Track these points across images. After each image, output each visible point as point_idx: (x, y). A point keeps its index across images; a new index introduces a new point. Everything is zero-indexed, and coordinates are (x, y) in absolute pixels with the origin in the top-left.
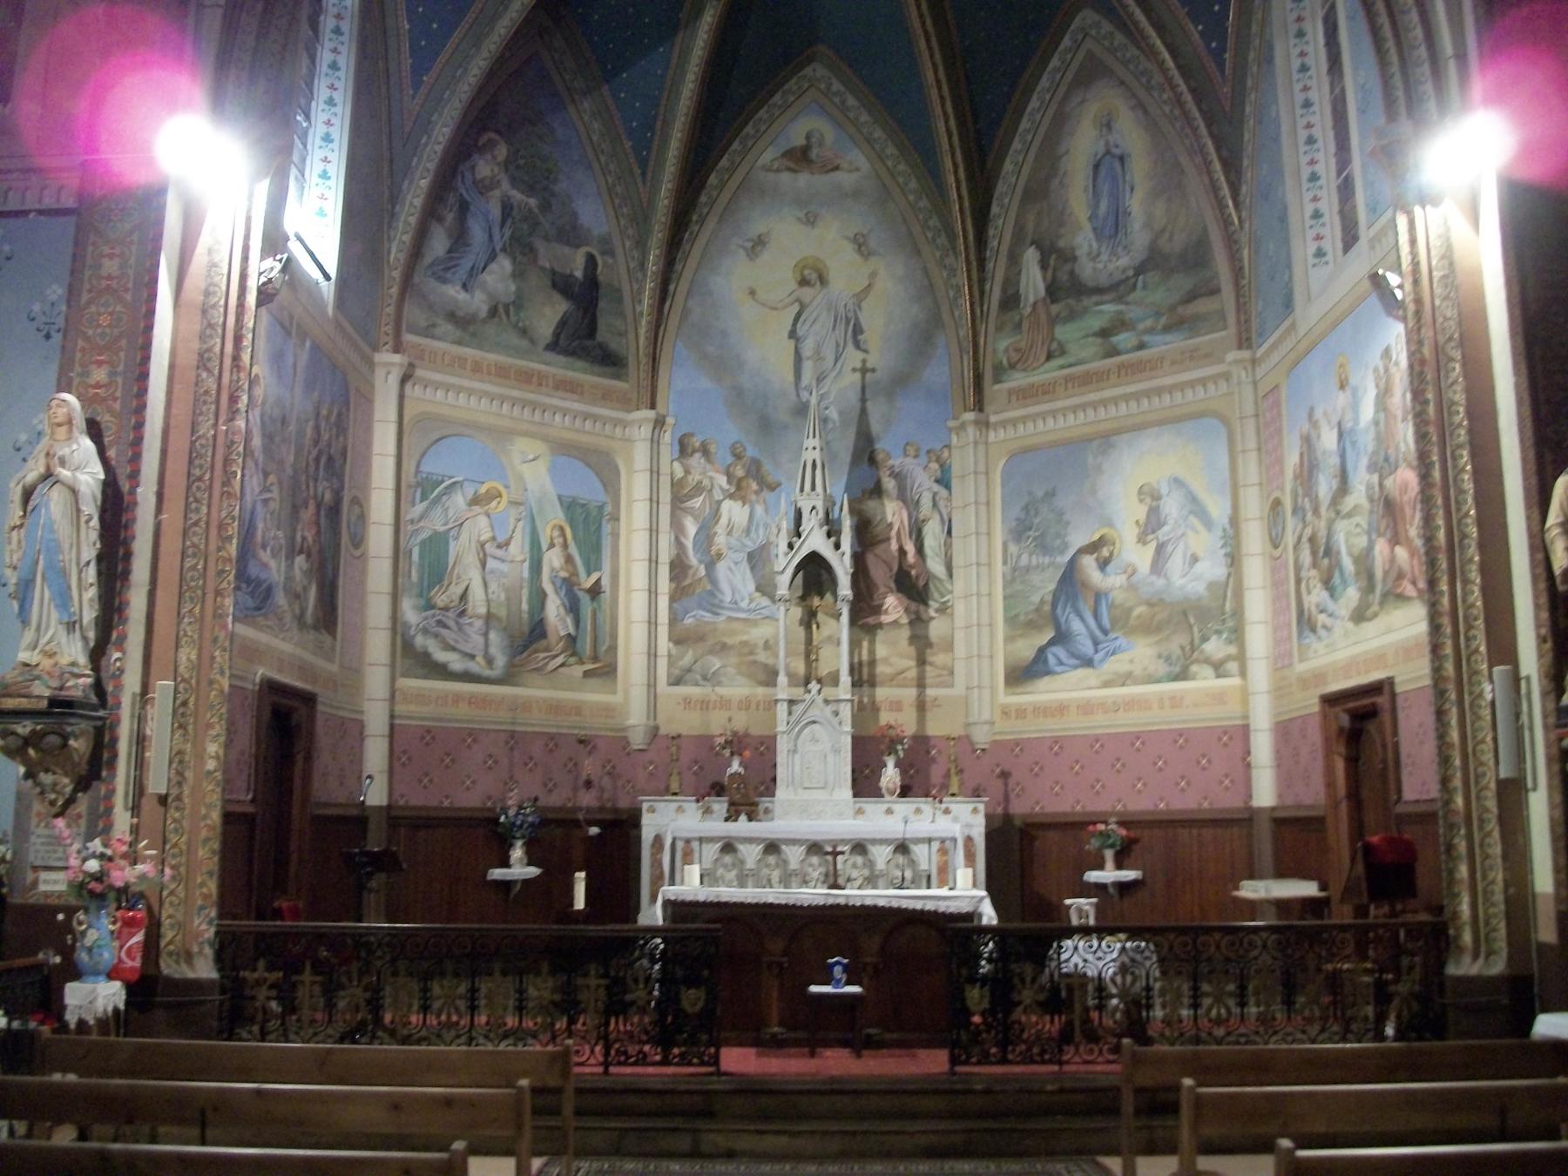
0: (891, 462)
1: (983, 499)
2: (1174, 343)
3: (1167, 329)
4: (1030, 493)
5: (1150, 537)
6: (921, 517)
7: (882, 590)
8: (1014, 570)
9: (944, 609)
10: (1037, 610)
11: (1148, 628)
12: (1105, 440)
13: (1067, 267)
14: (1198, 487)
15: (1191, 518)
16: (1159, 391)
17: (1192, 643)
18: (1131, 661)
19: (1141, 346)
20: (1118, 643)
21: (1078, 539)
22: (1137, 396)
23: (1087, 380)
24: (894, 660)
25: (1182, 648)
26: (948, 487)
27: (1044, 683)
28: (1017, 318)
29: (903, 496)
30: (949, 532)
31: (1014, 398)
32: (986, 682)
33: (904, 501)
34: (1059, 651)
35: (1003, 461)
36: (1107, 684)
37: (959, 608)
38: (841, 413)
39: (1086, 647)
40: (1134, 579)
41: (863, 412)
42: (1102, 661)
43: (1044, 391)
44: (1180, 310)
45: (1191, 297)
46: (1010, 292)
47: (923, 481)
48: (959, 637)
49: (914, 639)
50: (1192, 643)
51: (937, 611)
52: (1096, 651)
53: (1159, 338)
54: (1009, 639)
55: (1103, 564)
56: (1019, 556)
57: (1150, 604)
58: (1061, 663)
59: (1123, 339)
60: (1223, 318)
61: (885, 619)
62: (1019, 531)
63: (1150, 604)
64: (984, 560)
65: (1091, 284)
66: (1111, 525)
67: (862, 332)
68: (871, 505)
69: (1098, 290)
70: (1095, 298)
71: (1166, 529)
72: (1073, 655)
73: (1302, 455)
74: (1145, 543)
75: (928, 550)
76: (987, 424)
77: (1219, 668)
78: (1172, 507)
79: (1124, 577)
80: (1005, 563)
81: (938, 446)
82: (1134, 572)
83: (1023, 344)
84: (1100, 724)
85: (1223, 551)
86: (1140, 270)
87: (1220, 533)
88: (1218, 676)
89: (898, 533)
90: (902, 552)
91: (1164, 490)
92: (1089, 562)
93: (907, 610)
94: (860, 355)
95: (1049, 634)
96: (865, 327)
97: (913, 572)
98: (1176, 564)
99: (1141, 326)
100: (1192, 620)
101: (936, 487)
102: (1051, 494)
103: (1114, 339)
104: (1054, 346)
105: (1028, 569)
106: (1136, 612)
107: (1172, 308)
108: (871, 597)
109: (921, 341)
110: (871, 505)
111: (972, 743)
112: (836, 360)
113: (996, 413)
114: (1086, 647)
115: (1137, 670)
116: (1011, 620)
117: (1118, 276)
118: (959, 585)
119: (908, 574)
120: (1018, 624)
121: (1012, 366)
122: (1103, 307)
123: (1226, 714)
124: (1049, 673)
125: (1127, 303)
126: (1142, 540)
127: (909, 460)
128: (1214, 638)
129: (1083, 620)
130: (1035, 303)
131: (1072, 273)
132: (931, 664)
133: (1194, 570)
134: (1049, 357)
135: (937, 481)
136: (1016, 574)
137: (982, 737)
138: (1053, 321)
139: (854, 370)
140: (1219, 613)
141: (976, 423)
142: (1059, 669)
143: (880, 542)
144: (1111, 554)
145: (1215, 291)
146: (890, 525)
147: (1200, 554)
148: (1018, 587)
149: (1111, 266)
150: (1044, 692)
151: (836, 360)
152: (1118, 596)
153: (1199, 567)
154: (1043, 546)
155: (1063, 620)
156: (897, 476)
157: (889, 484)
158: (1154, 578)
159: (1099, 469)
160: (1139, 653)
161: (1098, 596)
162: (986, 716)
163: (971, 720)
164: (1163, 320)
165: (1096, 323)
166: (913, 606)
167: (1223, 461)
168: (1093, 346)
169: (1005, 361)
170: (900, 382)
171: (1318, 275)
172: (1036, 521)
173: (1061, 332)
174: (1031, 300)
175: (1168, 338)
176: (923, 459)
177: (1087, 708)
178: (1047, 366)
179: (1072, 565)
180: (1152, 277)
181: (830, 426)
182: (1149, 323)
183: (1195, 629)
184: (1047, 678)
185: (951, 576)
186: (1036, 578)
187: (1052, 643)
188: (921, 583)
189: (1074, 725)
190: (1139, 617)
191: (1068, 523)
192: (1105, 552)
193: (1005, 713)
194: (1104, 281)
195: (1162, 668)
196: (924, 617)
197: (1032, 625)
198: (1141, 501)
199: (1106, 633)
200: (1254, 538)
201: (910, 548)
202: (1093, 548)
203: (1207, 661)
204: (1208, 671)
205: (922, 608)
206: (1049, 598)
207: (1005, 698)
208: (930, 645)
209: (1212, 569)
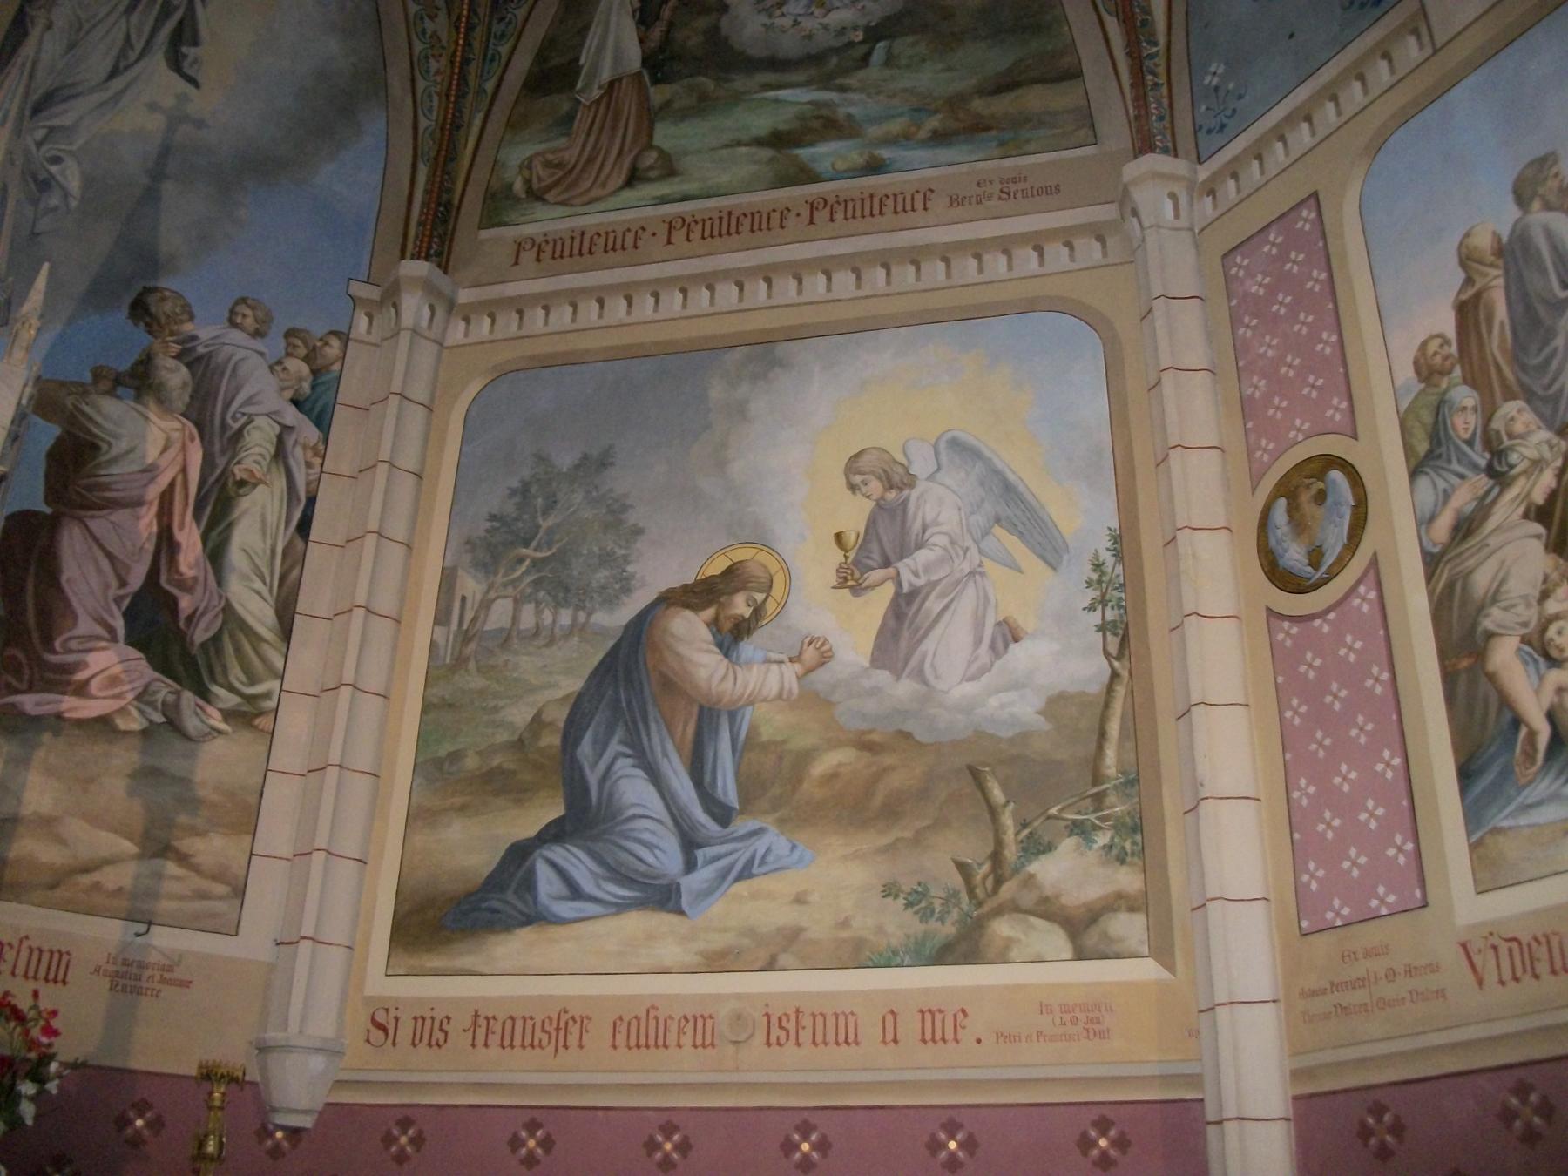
0: (188, 328)
1: (409, 460)
2: (964, 165)
3: (940, 138)
4: (541, 459)
5: (876, 575)
6: (239, 474)
7: (85, 625)
8: (465, 638)
9: (248, 715)
10: (519, 745)
11: (857, 808)
12: (765, 350)
13: (702, 23)
14: (1019, 462)
15: (997, 530)
16: (914, 256)
17: (996, 857)
18: (800, 900)
19: (875, 167)
20: (760, 845)
21: (662, 567)
22: (856, 265)
23: (724, 228)
24: (75, 828)
25: (962, 867)
26: (322, 422)
27: (511, 947)
28: (566, 107)
29: (203, 410)
30: (304, 528)
31: (528, 256)
32: (337, 930)
33: (199, 426)
34: (576, 860)
35: (474, 388)
36: (717, 962)
37: (294, 722)
38: (88, 182)
39: (666, 856)
40: (821, 677)
41: (151, 196)
42: (707, 893)
43: (617, 245)
44: (977, 104)
45: (1005, 84)
46: (555, 61)
47: (261, 391)
48: (280, 799)
49: (148, 775)
50: (996, 857)
51: (228, 715)
52: (690, 866)
54: (417, 817)
55: (731, 636)
56: (486, 605)
57: (866, 746)
58: (575, 892)
59: (824, 153)
60: (1087, 119)
61: (72, 706)
62: (495, 545)
63: (866, 746)
64: (386, 603)
65: (755, 52)
66: (763, 544)
67: (195, 42)
68: (112, 414)
69: (775, 64)
70: (769, 77)
71: (923, 556)
72: (618, 875)
73: (1468, 311)
74: (857, 589)
75: (235, 556)
76: (451, 306)
77: (1083, 930)
78: (941, 504)
79: (791, 672)
80: (441, 618)
81: (318, 329)
82: (825, 657)
83: (571, 156)
84: (678, 1078)
85: (1096, 618)
86: (875, 34)
87: (1087, 572)
88: (1080, 955)
89: (167, 498)
90: (166, 543)
91: (921, 466)
92: (689, 632)
93: (143, 697)
94: (181, 85)
95: (550, 810)
96: (204, 33)
97: (185, 603)
98: (950, 646)
99: (874, 131)
100: (997, 794)
101: (291, 415)
102: (596, 464)
103: (803, 153)
104: (650, 158)
105: (505, 638)
106: (820, 768)
107: (955, 103)
108: (48, 641)
109: (333, 109)
110: (112, 414)
111: (264, 1109)
112: (114, 73)
113: (477, 285)
114: (666, 856)
115: (818, 924)
116: (435, 767)
117: (825, 40)
118: (306, 659)
119: (172, 604)
120: (448, 779)
121: (536, 195)
122: (782, 94)
123: (1127, 1065)
124: (535, 917)
125: (842, 89)
126: (851, 580)
127: (237, 336)
128: (1068, 844)
129: (655, 777)
130: (611, 84)
131: (713, 33)
132: (183, 859)
133: (1011, 657)
134: (633, 179)
135: (295, 402)
136: (465, 651)
137: (299, 1090)
138: (650, 116)
139: (153, 107)
140: (1099, 772)
141: (429, 288)
142: (565, 909)
143: (116, 504)
144: (758, 611)
146: (151, 471)
147: (1026, 621)
148: (472, 680)
149: (808, 24)
150: (509, 973)
151: (114, 73)
152: (771, 722)
153: (1019, 656)
154: (556, 582)
155: (593, 779)
156: (198, 362)
157: (175, 376)
158: (883, 677)
159: (740, 412)
160: (826, 879)
161: (708, 716)
162: (323, 1026)
163: (273, 1035)
164: (934, 122)
165: (761, 122)
166: (164, 689)
167: (1096, 408)
168: (749, 163)
169: (518, 186)
170: (258, 168)
172: (545, 524)
173: (666, 135)
174: (606, 75)
175: (944, 154)
176: (275, 344)
177: (643, 1029)
178: (628, 194)
179: (640, 631)
180: (904, 46)
181: (54, 200)
182: (895, 126)
183: (1008, 821)
184: (525, 934)
185: (286, 632)
186: (526, 664)
187: (554, 833)
188: (200, 635)
189: (599, 1076)
190: (832, 777)
191: (637, 531)
192: (740, 606)
193: (381, 1026)
194: (789, 46)
195: (898, 923)
196: (191, 723)
197: (499, 785)
198: (853, 488)
199: (722, 815)
200: (1213, 574)
201: (190, 538)
202: (701, 594)
203: (1048, 909)
204: (1055, 940)
205: (188, 698)
206: (560, 715)
207: (386, 983)
208: (191, 802)
209: (1059, 657)
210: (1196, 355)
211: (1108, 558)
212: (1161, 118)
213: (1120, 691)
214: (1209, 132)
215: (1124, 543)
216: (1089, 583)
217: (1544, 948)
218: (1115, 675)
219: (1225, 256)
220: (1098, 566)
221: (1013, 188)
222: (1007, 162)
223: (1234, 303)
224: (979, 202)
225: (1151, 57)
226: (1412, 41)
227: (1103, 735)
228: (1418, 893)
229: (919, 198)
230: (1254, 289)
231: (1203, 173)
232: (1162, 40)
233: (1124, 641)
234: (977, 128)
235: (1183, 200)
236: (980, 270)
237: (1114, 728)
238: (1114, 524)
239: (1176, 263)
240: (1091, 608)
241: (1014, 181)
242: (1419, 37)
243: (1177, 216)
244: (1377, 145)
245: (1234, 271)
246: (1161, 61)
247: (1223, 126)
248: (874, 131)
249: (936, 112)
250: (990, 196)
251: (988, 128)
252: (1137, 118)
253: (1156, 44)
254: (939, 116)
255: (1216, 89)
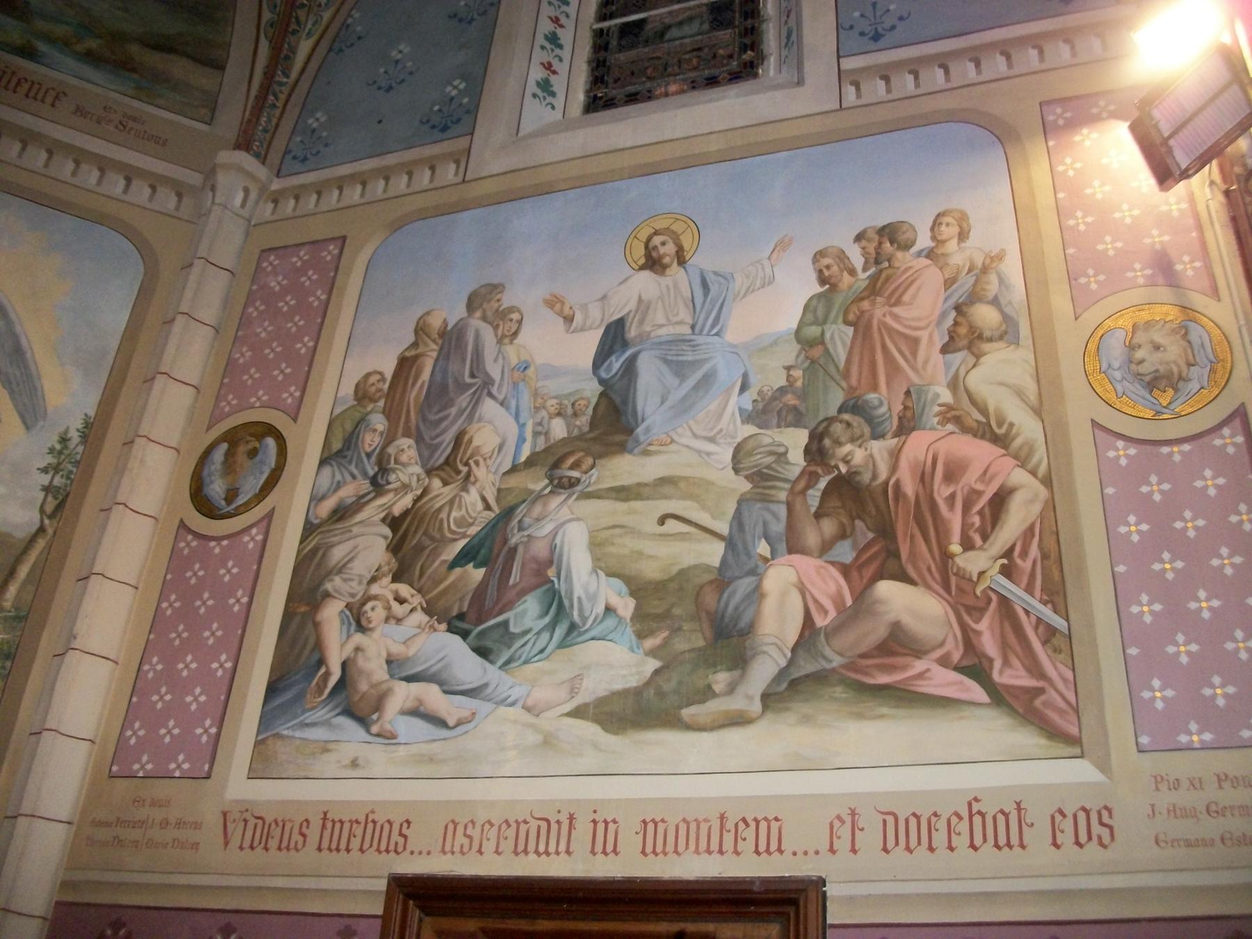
2: (100, 88)
3: (90, 57)
19: (28, 52)
44: (134, 49)
45: (165, 46)
53: (70, 62)
73: (406, 365)
85: (45, 479)
107: (117, 38)
145: (220, 67)
164: (93, 44)
167: (116, 317)
171: (536, 114)
175: (88, 71)
182: (60, 30)
200: (151, 480)
210: (210, 311)
211: (75, 436)
212: (265, 131)
213: (41, 543)
214: (294, 158)
215: (93, 431)
216: (51, 450)
217: (279, 830)
218: (42, 529)
219: (263, 251)
220: (64, 440)
221: (131, 124)
222: (136, 103)
223: (255, 287)
224: (99, 122)
225: (281, 84)
226: (453, 166)
227: (12, 573)
228: (207, 767)
229: (52, 94)
230: (273, 284)
231: (276, 185)
232: (294, 74)
233: (60, 507)
234: (124, 66)
235: (253, 195)
236: (74, 174)
237: (23, 571)
238: (92, 413)
239: (226, 240)
240: (45, 470)
241: (135, 119)
242: (458, 167)
243: (243, 206)
244: (397, 225)
245: (265, 264)
246: (286, 90)
247: (305, 159)
248: (40, 25)
249: (99, 37)
250: (110, 121)
251: (133, 70)
252: (249, 121)
253: (288, 77)
254: (99, 41)
255: (314, 131)
